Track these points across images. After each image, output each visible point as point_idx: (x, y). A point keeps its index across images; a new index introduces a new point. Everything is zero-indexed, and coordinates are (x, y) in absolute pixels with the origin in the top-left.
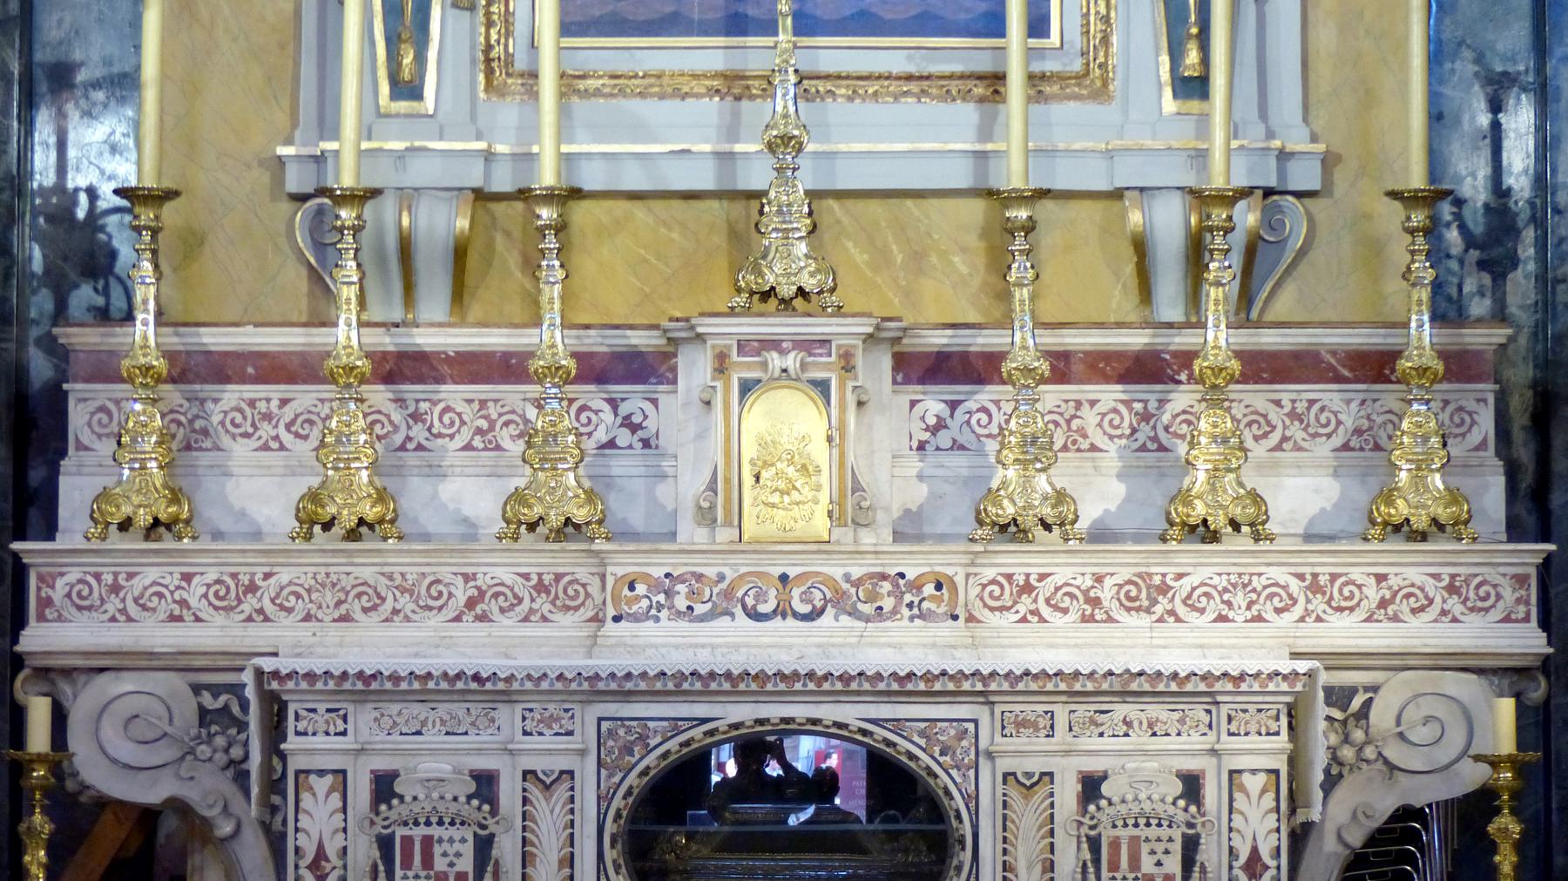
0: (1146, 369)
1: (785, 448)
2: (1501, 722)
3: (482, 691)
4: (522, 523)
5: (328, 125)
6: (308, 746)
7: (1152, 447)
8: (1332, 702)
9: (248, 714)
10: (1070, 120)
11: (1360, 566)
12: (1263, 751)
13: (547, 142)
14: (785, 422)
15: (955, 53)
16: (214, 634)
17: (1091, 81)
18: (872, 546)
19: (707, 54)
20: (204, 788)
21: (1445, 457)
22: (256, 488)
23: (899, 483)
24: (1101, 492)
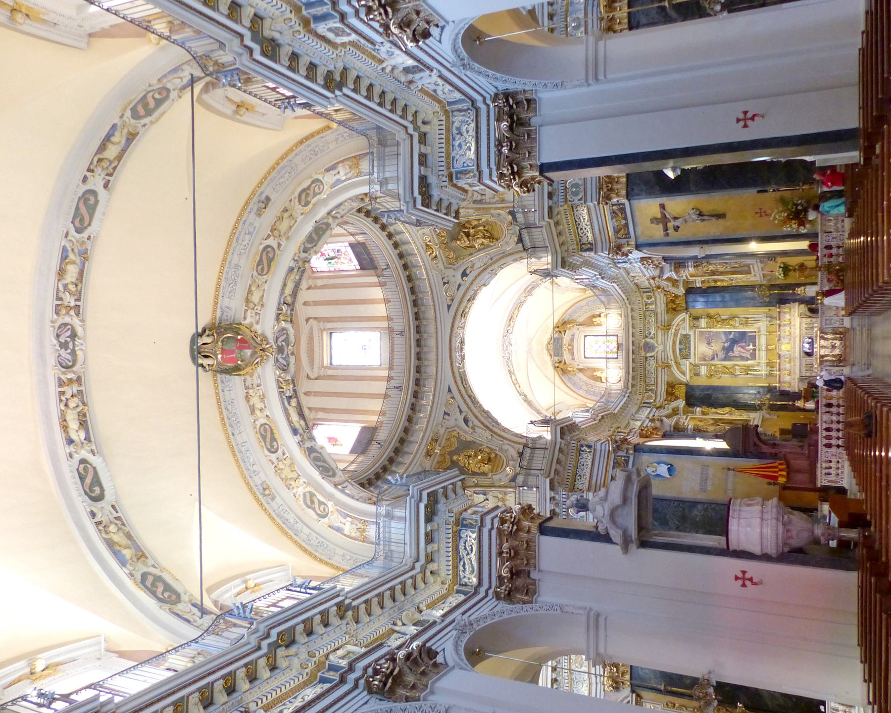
0: (780, 326)
1: (785, 347)
2: (802, 306)
3: (800, 365)
4: (790, 362)
5: (761, 375)
6: (804, 374)
7: (785, 325)
8: (801, 316)
9: (802, 379)
10: (762, 329)
11: (792, 313)
12: (804, 320)
13: (764, 361)
14: (783, 347)
15: (757, 337)
16: (797, 380)
17: (759, 328)
18: (792, 342)
19: (757, 352)
20: (807, 381)
21: (785, 308)
22: (787, 378)
23: (787, 340)
24: (788, 328)
